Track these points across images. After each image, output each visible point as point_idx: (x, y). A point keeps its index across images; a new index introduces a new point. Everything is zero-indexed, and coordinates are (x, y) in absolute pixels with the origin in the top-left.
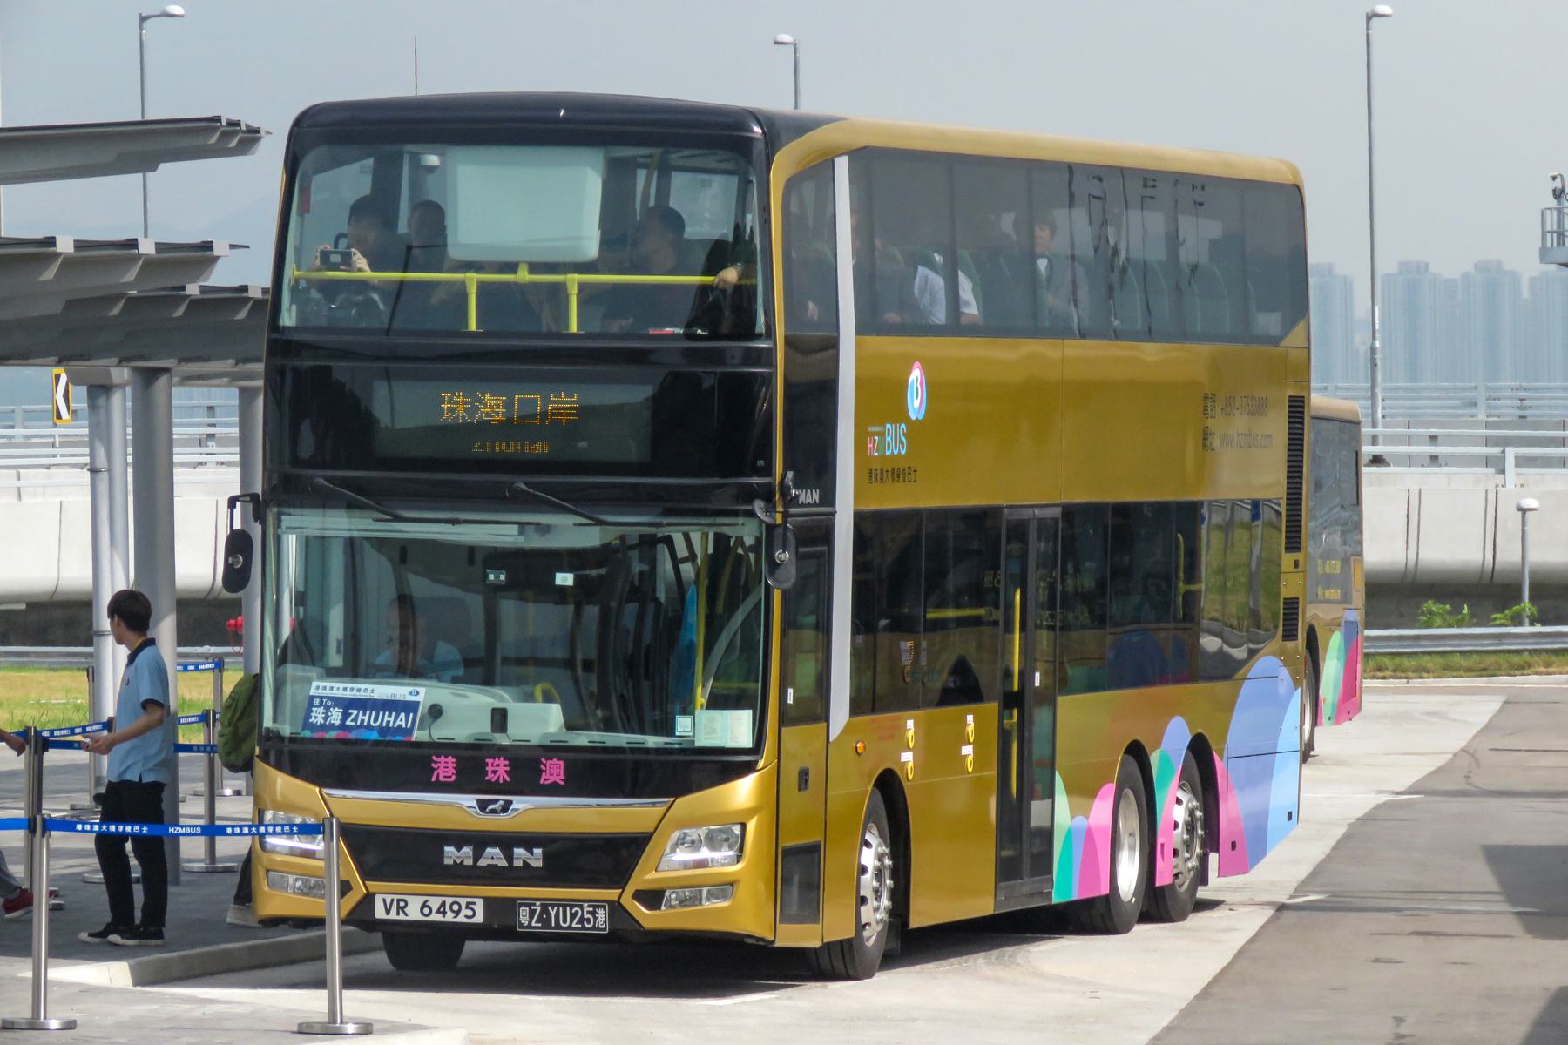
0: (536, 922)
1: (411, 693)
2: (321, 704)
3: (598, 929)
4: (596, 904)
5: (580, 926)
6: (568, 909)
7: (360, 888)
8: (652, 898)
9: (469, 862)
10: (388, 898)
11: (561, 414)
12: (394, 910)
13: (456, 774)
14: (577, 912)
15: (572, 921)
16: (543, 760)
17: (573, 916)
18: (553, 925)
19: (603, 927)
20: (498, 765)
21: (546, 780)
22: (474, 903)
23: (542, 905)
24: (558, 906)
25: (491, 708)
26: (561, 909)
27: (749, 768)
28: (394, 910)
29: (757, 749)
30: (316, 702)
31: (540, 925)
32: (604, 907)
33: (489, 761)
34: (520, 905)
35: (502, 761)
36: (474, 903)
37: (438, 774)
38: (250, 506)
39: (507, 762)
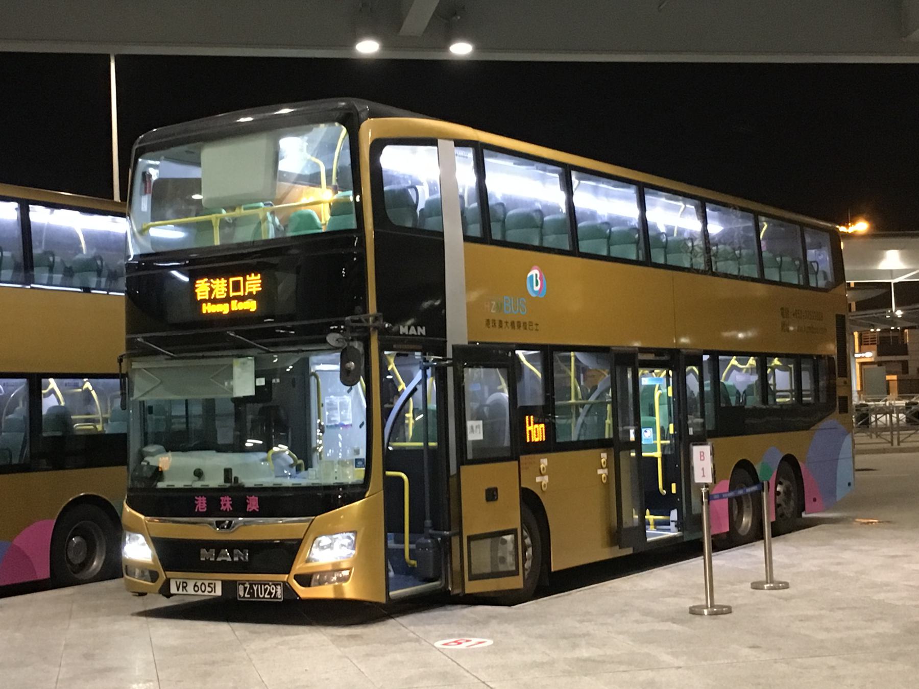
0: (248, 594)
3: (277, 598)
4: (276, 584)
6: (263, 586)
7: (163, 576)
8: (305, 580)
9: (212, 559)
11: (252, 288)
14: (267, 588)
16: (248, 497)
18: (256, 596)
23: (250, 584)
24: (258, 584)
25: (223, 469)
26: (259, 586)
31: (249, 596)
32: (280, 585)
33: (222, 498)
34: (239, 584)
35: (228, 499)
39: (230, 499)
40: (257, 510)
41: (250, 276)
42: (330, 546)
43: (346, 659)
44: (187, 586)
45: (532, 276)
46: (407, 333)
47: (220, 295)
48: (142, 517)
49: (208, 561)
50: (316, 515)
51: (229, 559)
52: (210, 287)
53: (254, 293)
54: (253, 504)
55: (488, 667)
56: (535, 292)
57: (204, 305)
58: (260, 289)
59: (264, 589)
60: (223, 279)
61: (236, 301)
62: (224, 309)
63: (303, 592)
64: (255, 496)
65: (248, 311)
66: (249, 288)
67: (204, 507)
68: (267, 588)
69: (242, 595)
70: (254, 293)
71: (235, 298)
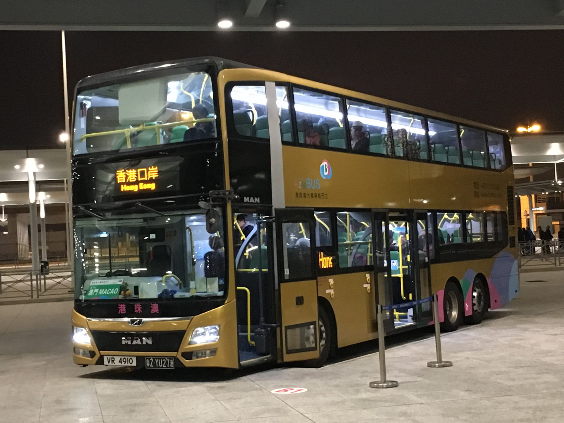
0: (152, 365)
1: (119, 281)
2: (93, 289)
3: (171, 367)
5: (165, 366)
6: (161, 360)
8: (188, 355)
9: (129, 342)
10: (109, 357)
11: (152, 175)
12: (111, 362)
13: (126, 311)
14: (164, 361)
15: (163, 364)
16: (152, 304)
17: (163, 362)
18: (157, 366)
19: (172, 367)
20: (138, 307)
21: (153, 311)
23: (153, 359)
24: (158, 359)
28: (111, 362)
29: (225, 296)
30: (91, 288)
31: (153, 366)
32: (172, 359)
34: (147, 359)
37: (120, 311)
38: (77, 219)
39: (141, 305)
40: (158, 312)
41: (151, 168)
42: (203, 334)
43: (217, 401)
44: (114, 360)
45: (323, 166)
46: (248, 202)
47: (132, 180)
48: (85, 318)
49: (127, 344)
50: (195, 316)
51: (140, 343)
52: (126, 174)
53: (154, 178)
55: (304, 405)
56: (325, 176)
57: (122, 186)
58: (158, 176)
59: (163, 362)
60: (134, 170)
61: (143, 183)
62: (135, 188)
63: (187, 363)
64: (157, 304)
65: (150, 189)
66: (150, 175)
68: (164, 361)
69: (149, 366)
70: (154, 178)
71: (141, 181)
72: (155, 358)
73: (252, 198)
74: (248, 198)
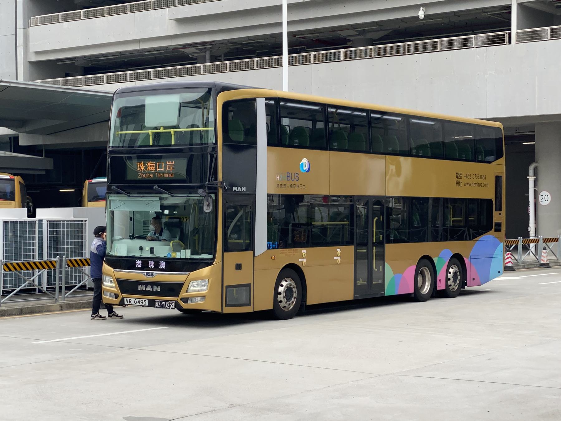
4: (172, 301)
8: (185, 300)
10: (127, 299)
12: (128, 302)
13: (142, 265)
15: (167, 306)
16: (160, 262)
17: (168, 304)
21: (161, 267)
22: (146, 301)
23: (160, 301)
27: (211, 264)
28: (128, 302)
31: (160, 307)
32: (174, 302)
33: (149, 262)
34: (156, 301)
35: (152, 262)
36: (146, 301)
39: (153, 262)
40: (164, 268)
46: (236, 190)
49: (141, 290)
50: (191, 271)
51: (151, 290)
54: (162, 265)
64: (164, 261)
67: (140, 265)
72: (162, 301)
73: (239, 188)
74: (236, 187)
